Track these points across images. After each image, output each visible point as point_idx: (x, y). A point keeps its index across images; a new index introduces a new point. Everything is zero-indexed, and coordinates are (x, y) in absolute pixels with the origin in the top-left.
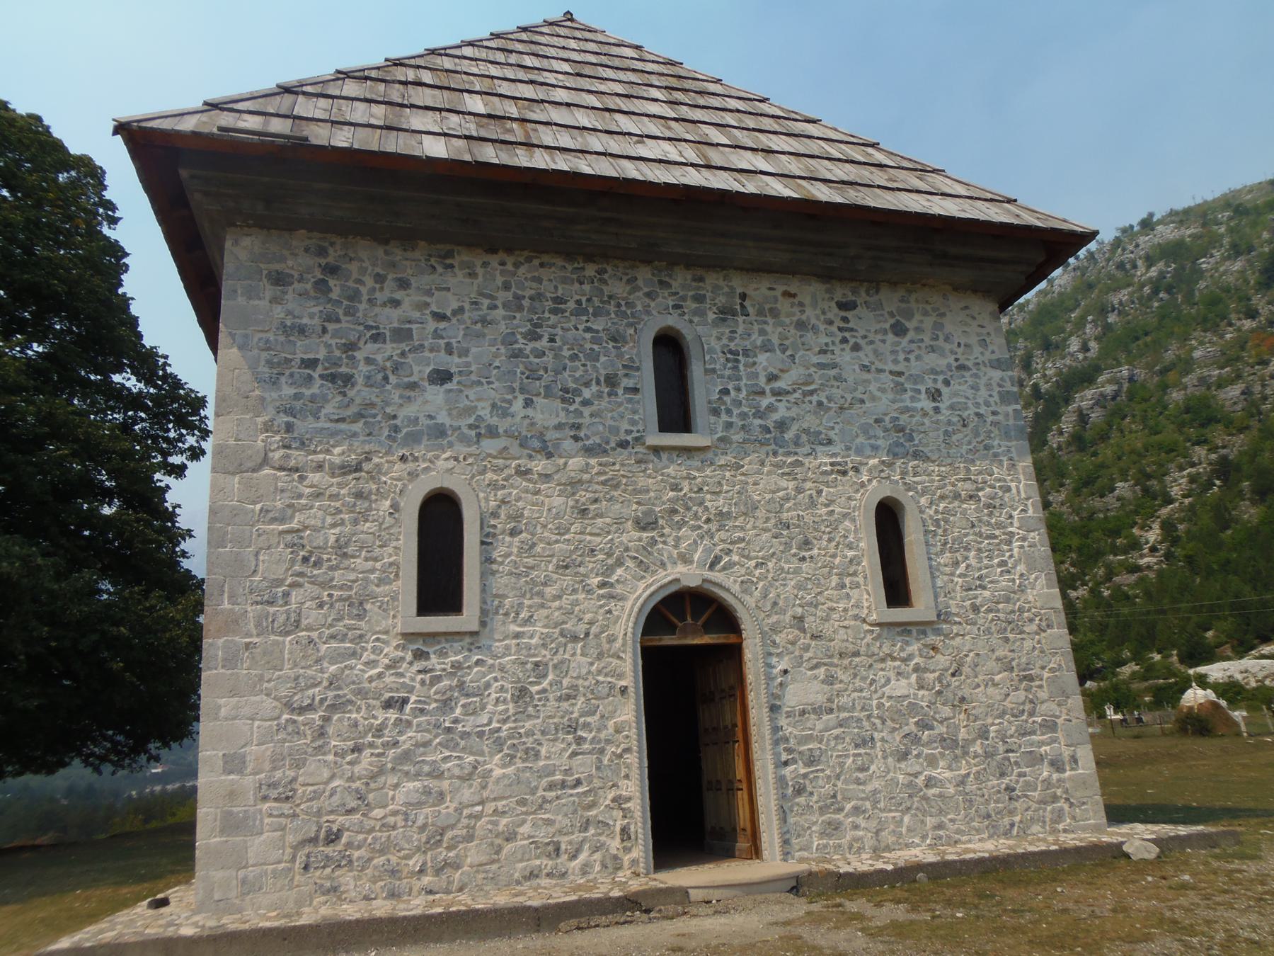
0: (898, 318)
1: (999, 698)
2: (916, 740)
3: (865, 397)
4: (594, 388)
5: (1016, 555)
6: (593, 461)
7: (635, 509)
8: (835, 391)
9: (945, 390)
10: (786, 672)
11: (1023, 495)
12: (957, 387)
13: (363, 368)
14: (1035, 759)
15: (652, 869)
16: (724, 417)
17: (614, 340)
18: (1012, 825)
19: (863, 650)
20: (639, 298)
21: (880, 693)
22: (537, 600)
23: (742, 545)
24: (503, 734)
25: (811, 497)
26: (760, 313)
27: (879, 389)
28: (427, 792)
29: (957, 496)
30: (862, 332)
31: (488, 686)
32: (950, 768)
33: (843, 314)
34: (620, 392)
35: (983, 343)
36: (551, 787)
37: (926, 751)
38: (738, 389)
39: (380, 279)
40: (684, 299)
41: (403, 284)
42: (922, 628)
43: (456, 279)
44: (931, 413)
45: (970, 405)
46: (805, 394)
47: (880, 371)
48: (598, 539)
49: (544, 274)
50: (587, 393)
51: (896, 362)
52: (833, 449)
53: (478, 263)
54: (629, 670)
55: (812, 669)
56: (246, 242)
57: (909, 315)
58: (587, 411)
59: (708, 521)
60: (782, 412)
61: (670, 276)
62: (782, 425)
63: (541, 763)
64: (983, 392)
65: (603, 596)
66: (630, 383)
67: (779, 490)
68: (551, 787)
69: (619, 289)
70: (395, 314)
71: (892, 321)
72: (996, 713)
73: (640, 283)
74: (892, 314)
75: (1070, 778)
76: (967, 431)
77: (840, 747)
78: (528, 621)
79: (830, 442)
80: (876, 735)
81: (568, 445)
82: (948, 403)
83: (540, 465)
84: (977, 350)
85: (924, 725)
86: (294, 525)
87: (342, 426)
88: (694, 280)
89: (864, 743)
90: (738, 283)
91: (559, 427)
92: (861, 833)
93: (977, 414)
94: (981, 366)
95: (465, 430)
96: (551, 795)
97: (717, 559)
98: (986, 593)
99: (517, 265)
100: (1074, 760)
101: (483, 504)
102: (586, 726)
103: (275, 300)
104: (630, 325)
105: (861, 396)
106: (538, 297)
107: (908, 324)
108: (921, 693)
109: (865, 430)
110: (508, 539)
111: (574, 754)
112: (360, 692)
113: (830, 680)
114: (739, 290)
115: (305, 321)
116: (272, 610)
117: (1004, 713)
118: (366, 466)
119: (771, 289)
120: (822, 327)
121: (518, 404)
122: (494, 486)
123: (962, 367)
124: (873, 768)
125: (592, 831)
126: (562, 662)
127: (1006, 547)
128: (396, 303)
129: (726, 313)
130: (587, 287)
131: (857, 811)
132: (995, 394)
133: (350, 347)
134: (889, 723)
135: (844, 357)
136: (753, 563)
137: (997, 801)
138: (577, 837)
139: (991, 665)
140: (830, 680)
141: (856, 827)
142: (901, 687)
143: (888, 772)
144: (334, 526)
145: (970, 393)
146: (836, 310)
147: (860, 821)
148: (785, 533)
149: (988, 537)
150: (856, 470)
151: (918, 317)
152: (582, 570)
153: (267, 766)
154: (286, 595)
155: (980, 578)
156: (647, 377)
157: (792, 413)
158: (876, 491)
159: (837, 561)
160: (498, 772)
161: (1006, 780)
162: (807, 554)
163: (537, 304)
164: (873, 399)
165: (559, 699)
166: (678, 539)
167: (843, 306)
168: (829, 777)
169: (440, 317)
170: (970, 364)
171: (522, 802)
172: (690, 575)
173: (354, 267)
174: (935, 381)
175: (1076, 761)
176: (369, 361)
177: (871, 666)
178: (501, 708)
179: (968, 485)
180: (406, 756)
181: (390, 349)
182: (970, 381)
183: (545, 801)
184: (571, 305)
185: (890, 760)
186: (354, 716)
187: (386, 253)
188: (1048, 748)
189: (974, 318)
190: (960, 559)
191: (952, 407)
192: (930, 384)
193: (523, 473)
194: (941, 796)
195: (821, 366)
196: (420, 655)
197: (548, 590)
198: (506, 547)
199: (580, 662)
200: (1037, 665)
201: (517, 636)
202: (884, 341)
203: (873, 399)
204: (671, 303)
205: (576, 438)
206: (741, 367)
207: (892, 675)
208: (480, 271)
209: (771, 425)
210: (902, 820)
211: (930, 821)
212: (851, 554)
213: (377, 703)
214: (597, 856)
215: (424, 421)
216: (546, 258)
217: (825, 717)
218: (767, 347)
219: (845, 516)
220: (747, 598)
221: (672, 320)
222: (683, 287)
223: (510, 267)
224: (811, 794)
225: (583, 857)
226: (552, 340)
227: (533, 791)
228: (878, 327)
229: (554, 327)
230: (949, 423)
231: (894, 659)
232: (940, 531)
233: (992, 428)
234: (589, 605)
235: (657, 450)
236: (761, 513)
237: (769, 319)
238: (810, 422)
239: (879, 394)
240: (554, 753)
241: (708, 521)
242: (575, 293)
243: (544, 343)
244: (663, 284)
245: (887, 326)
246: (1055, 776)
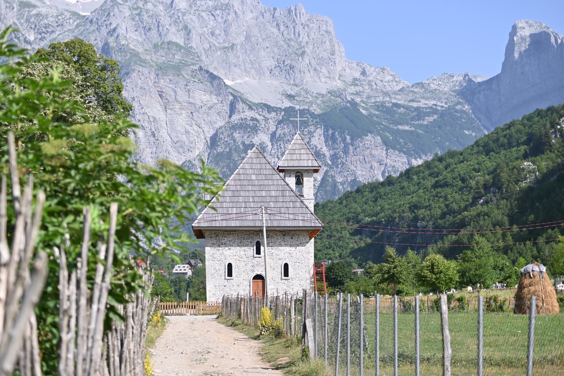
7: (252, 265)
35: (305, 239)
41: (225, 237)
62: (272, 253)
103: (211, 240)
106: (241, 237)
109: (284, 254)
121: (238, 253)
123: (301, 243)
169: (229, 241)
218: (272, 242)
221: (258, 240)
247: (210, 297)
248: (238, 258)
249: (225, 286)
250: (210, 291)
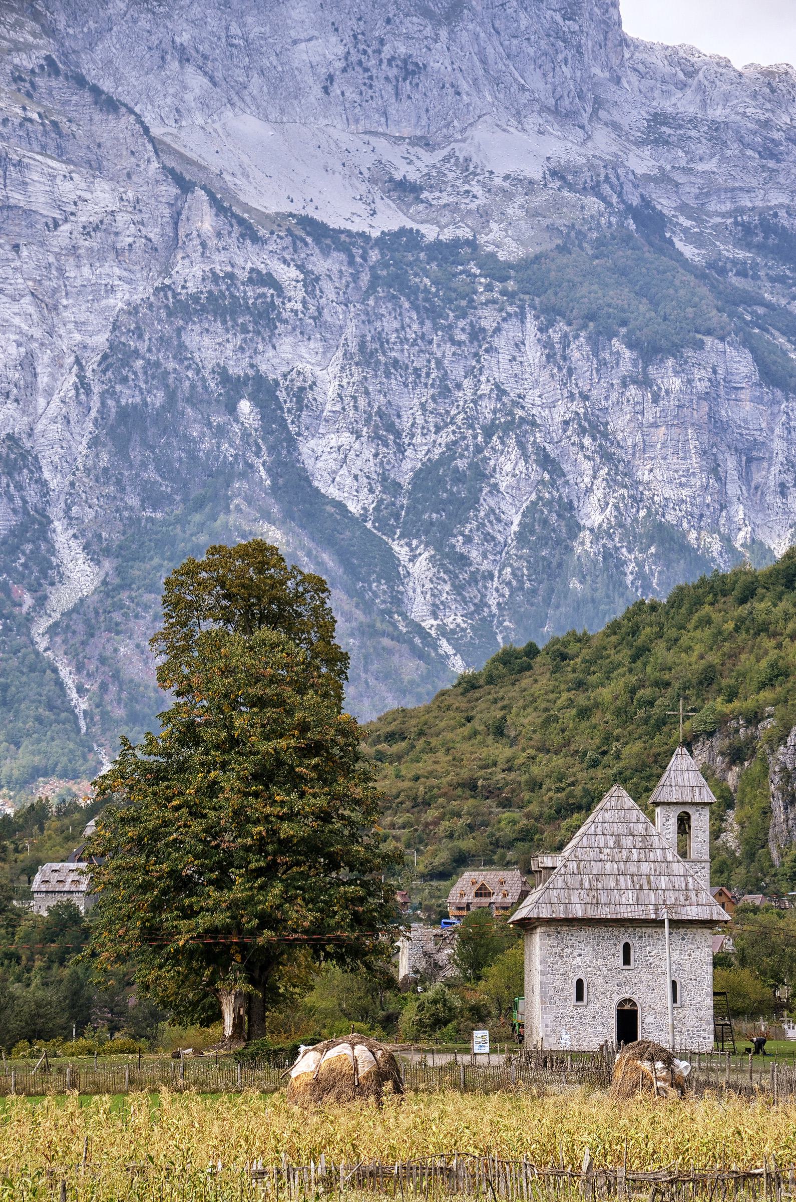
54: (614, 1013)
129: (641, 937)
156: (621, 954)
172: (627, 996)
199: (605, 1012)
234: (607, 1001)
240: (600, 1028)
242: (607, 935)
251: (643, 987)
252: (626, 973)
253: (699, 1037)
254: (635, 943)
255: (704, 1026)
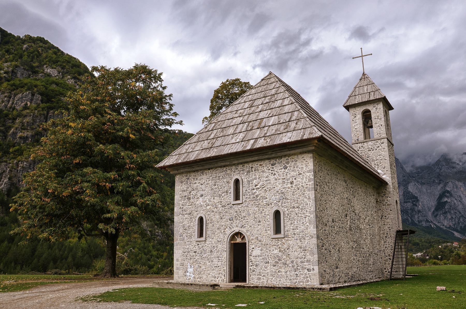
0: (286, 164)
1: (297, 254)
2: (278, 263)
3: (275, 186)
4: (224, 194)
5: (307, 220)
6: (223, 208)
8: (269, 186)
9: (295, 181)
10: (253, 248)
11: (311, 206)
12: (298, 179)
13: (192, 196)
14: (303, 268)
15: (228, 282)
16: (246, 196)
17: (228, 183)
18: (296, 282)
19: (269, 244)
20: (232, 173)
21: (271, 253)
22: (214, 235)
23: (247, 223)
24: (209, 258)
25: (261, 211)
26: (255, 170)
27: (279, 184)
28: (199, 266)
29: (294, 207)
30: (276, 170)
31: (207, 250)
32: (284, 269)
33: (272, 167)
34: (228, 194)
36: (215, 267)
37: (280, 265)
38: (249, 189)
39: (194, 179)
40: (240, 171)
42: (282, 239)
43: (204, 177)
44: (291, 187)
45: (300, 184)
46: (262, 188)
47: (279, 179)
48: (223, 223)
49: (217, 172)
50: (223, 195)
51: (283, 176)
52: (266, 200)
53: (207, 172)
55: (258, 248)
56: (178, 176)
57: (288, 163)
58: (223, 198)
59: (242, 218)
60: (258, 193)
61: (238, 167)
62: (257, 196)
63: (214, 263)
64: (305, 180)
65: (224, 234)
66: (229, 192)
67: (255, 210)
68: (215, 267)
69: (229, 172)
70: (195, 185)
71: (284, 166)
72: (296, 258)
73: (233, 170)
74: (284, 164)
75: (312, 273)
76: (299, 191)
77: (262, 263)
78: (213, 239)
79: (266, 198)
80: (269, 261)
81: (220, 206)
82: (295, 184)
83: (215, 210)
84: (305, 168)
85: (279, 260)
86: (184, 224)
87: (189, 207)
88: (242, 166)
89: (267, 263)
90: (250, 165)
91: (218, 202)
92: (264, 280)
93: (302, 186)
94: (305, 173)
95: (205, 205)
96: (215, 268)
97: (243, 226)
98: (298, 231)
99: (213, 171)
100: (313, 269)
101: (207, 218)
102: (220, 257)
104: (231, 179)
105: (274, 186)
107: (287, 166)
108: (280, 253)
110: (210, 224)
111: (218, 262)
112: (191, 250)
113: (261, 250)
114: (251, 166)
115: (185, 189)
116: (181, 237)
117: (298, 258)
118: (192, 213)
119: (257, 165)
120: (267, 171)
122: (208, 215)
123: (300, 174)
124: (268, 268)
125: (220, 274)
126: (217, 246)
127: (304, 219)
128: (196, 183)
129: (249, 172)
130: (224, 173)
131: (264, 276)
132: (307, 180)
133: (190, 193)
134: (273, 259)
135: (272, 177)
136: (249, 226)
137: (294, 277)
138: (218, 275)
139: (296, 247)
140: (261, 250)
141: (264, 279)
142: (276, 252)
143: (271, 269)
144: (188, 223)
145: (301, 180)
146: (271, 166)
147: (264, 278)
148: (255, 220)
149: (300, 217)
150: (271, 204)
151: (290, 163)
152: (221, 229)
153: (181, 261)
154: (183, 235)
155: (297, 227)
157: (259, 193)
158: (275, 209)
159: (265, 225)
160: (208, 264)
161: (296, 273)
162: (259, 224)
163: (216, 178)
164: (277, 186)
165: (216, 252)
166: (236, 222)
167: (272, 165)
168: (259, 269)
170: (302, 173)
171: (211, 269)
172: (237, 230)
173: (191, 177)
174: (293, 179)
175: (314, 270)
176: (192, 194)
177: (270, 247)
178: (208, 253)
179: (297, 204)
180: (196, 261)
181: (195, 192)
182: (301, 177)
183: (214, 269)
184: (221, 177)
185: (272, 266)
186: (190, 254)
187: (195, 174)
188: (307, 266)
189: (305, 160)
190: (293, 223)
191: (295, 185)
192: (291, 180)
193: (213, 212)
194: (281, 274)
195: (266, 181)
196: (198, 244)
197: (216, 233)
198: (210, 225)
200: (308, 247)
201: (211, 241)
202: (281, 172)
203: (277, 186)
204: (238, 173)
205: (221, 204)
206: (250, 184)
207: (274, 249)
208: (207, 174)
209: (255, 196)
210: (273, 278)
211: (278, 279)
212: (268, 223)
213: (193, 252)
214: (221, 279)
215: (199, 204)
216: (217, 169)
217: (260, 257)
218: (255, 179)
219: (268, 215)
220: (247, 233)
222: (240, 169)
223: (212, 172)
224: (256, 272)
225: (219, 279)
226: (218, 185)
227: (212, 267)
228: (280, 168)
229: (218, 182)
230: (294, 190)
231: (275, 246)
232: (289, 216)
233: (305, 189)
234: (222, 236)
235: (233, 205)
236: (251, 216)
237: (257, 172)
238: (263, 194)
239: (278, 185)
240: (215, 261)
241: (242, 218)
243: (217, 186)
244: (237, 169)
245: (282, 167)
246: (308, 272)
247: (178, 269)
248: (212, 208)
249: (195, 252)
250: (177, 260)
251: (251, 220)
252: (236, 208)
253: (303, 268)
254: (243, 177)
255: (309, 257)
